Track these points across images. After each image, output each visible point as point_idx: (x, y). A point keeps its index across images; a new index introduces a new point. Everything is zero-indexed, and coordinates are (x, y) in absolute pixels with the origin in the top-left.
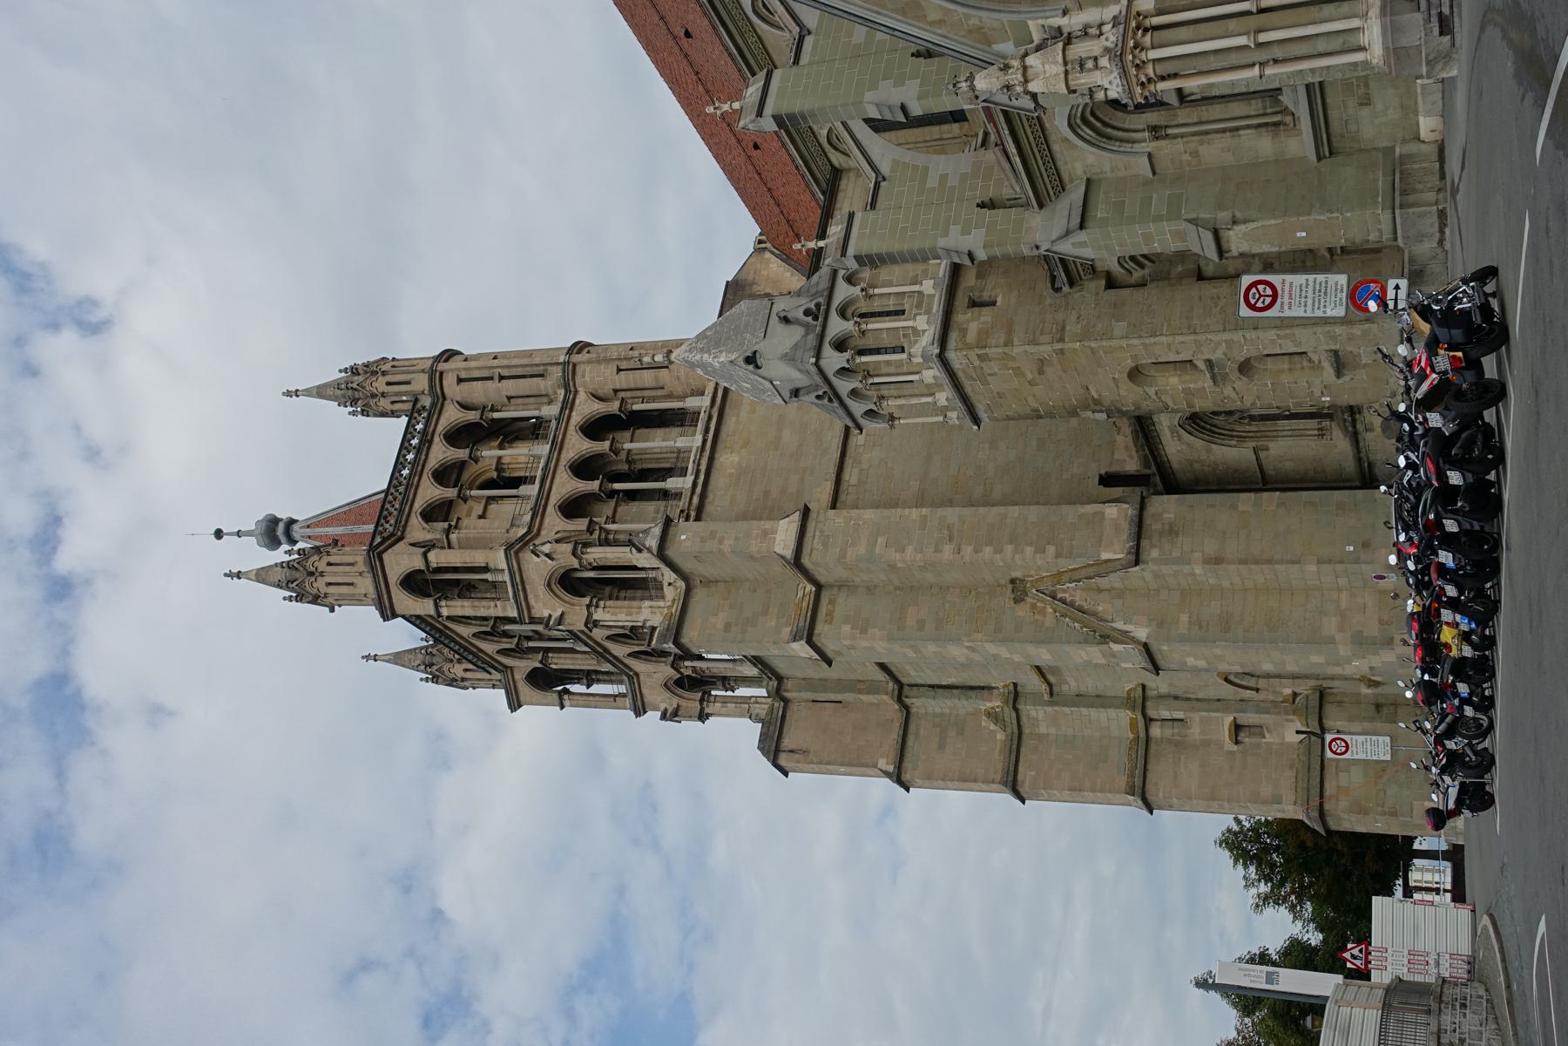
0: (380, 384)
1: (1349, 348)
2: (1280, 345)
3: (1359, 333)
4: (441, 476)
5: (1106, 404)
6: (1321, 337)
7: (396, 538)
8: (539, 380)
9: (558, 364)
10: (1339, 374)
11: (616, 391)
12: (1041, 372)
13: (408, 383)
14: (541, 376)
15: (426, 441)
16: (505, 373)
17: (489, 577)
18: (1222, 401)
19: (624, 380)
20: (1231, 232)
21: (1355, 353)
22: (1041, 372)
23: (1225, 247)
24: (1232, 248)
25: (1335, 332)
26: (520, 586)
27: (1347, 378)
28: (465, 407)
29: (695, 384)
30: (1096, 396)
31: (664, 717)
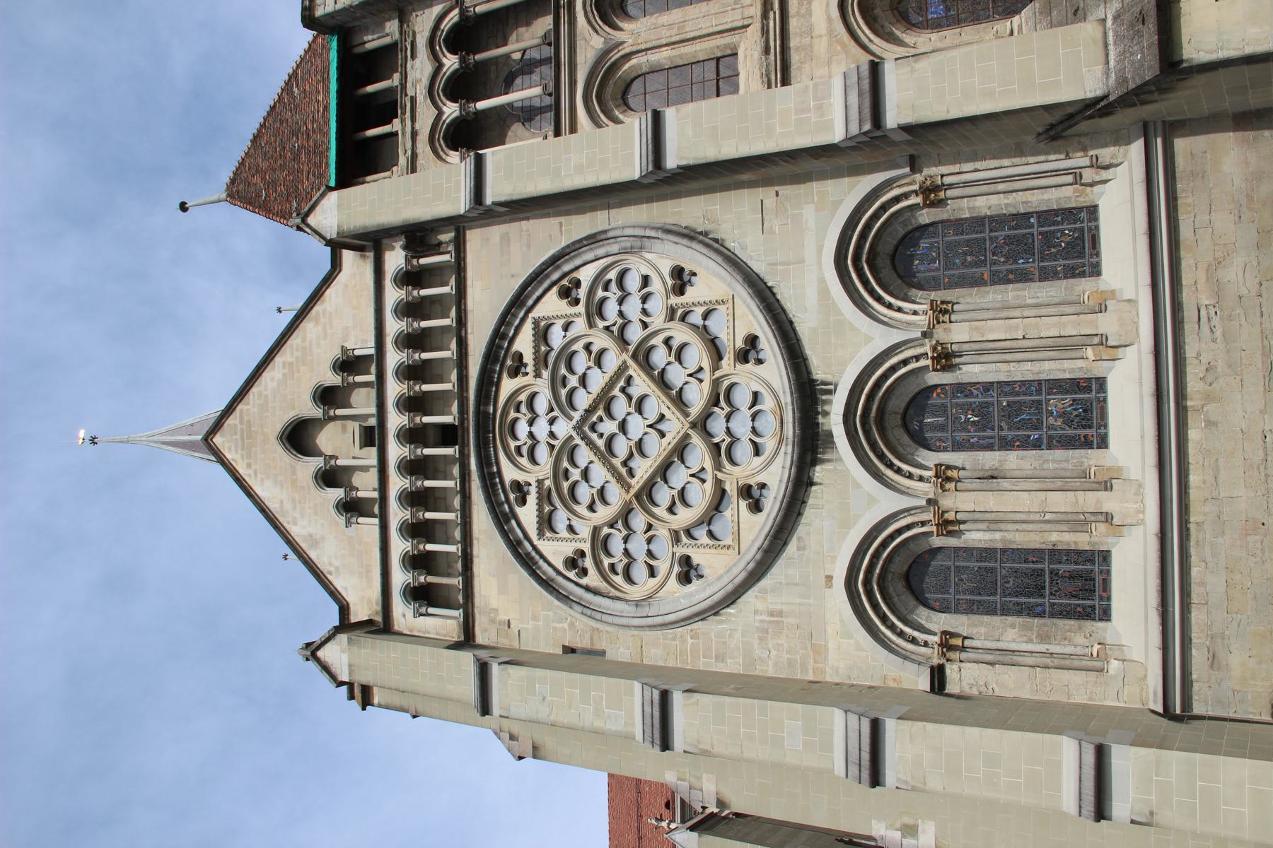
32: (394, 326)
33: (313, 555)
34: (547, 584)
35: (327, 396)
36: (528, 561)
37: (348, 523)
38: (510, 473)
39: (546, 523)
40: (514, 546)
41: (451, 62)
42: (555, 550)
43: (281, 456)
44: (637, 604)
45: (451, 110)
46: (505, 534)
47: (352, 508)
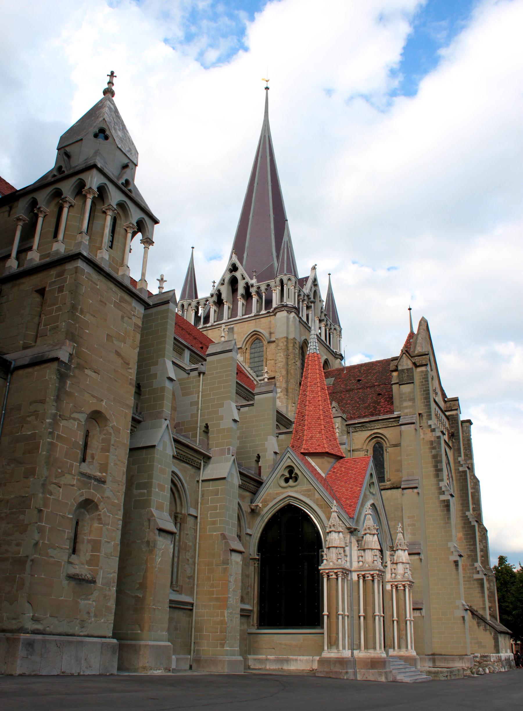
1: (96, 594)
2: (109, 542)
3: (109, 604)
5: (77, 371)
6: (112, 576)
10: (71, 577)
12: (118, 353)
18: (60, 468)
20: (170, 542)
21: (90, 597)
22: (118, 353)
23: (162, 533)
24: (160, 538)
25: (113, 587)
27: (65, 583)
30: (86, 370)
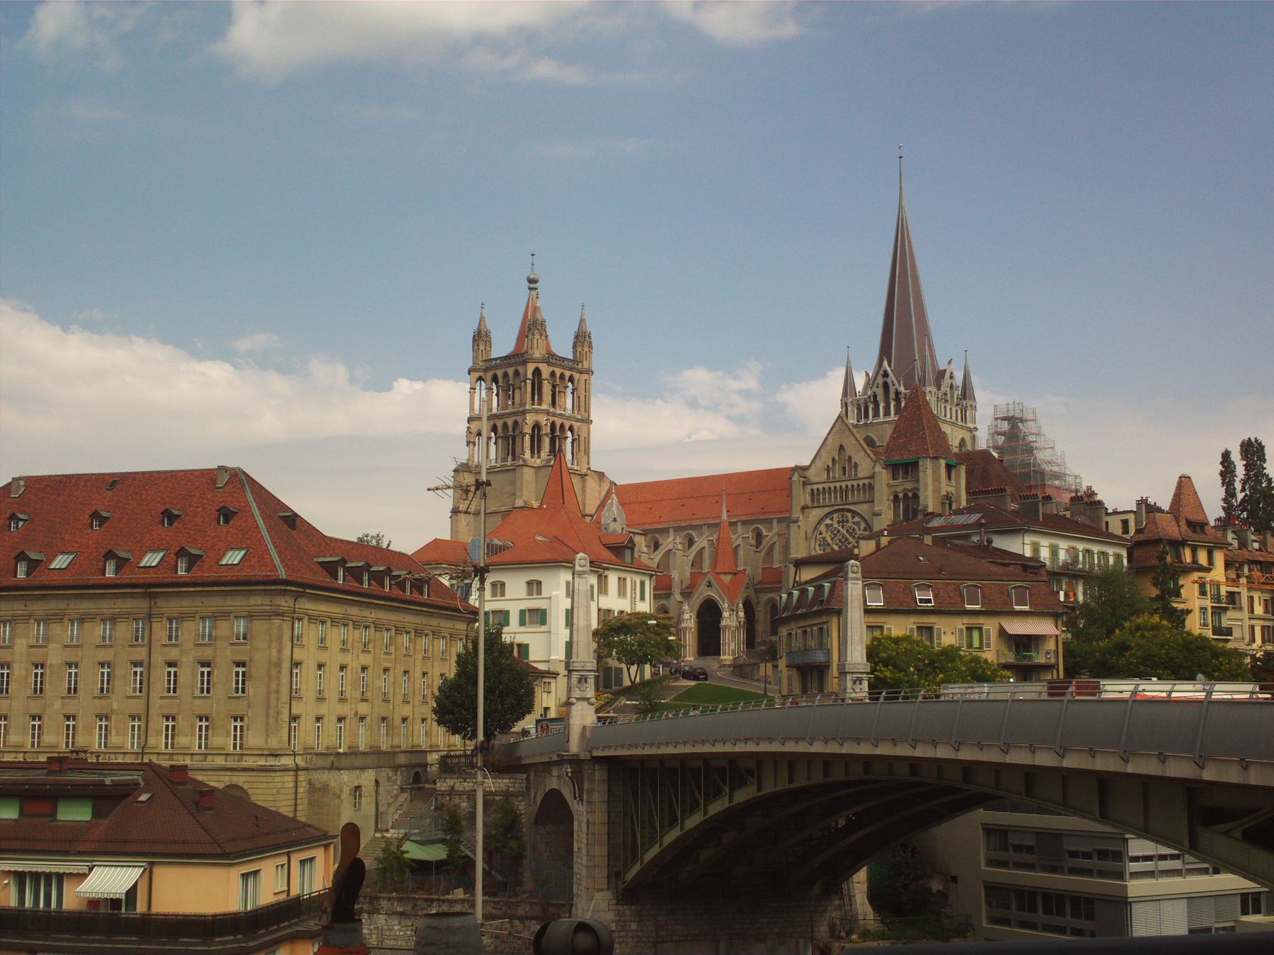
0: (586, 349)
4: (562, 376)
7: (549, 363)
8: (584, 410)
9: (589, 416)
11: (579, 436)
13: (586, 360)
14: (585, 410)
15: (571, 369)
16: (587, 397)
17: (536, 397)
19: (582, 439)
26: (537, 411)
28: (578, 380)
29: (580, 463)
31: (468, 428)
32: (861, 483)
33: (818, 458)
34: (815, 528)
35: (850, 457)
36: (819, 523)
37: (825, 469)
38: (835, 516)
39: (827, 526)
40: (821, 519)
41: (910, 494)
42: (822, 528)
43: (837, 446)
44: (815, 548)
45: (901, 496)
46: (823, 517)
47: (828, 469)
